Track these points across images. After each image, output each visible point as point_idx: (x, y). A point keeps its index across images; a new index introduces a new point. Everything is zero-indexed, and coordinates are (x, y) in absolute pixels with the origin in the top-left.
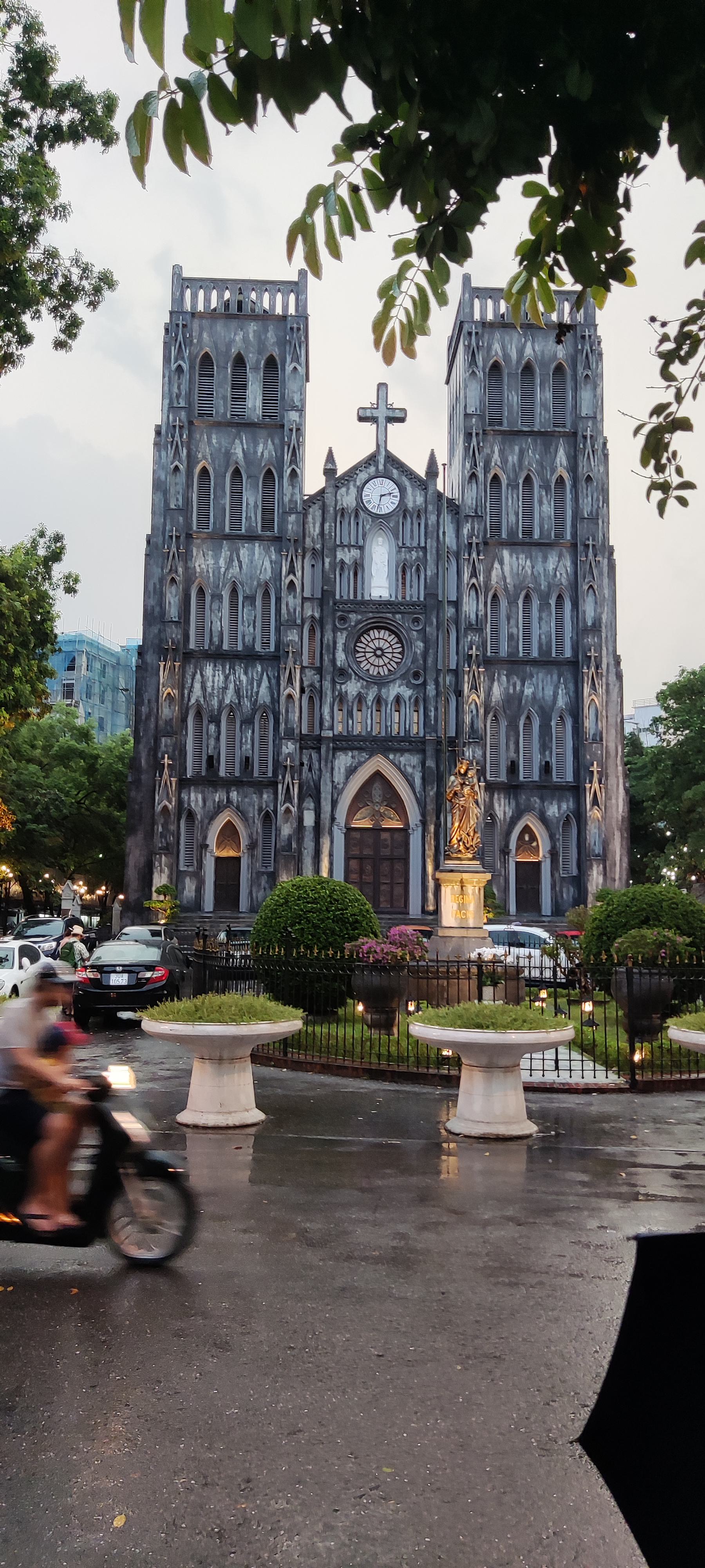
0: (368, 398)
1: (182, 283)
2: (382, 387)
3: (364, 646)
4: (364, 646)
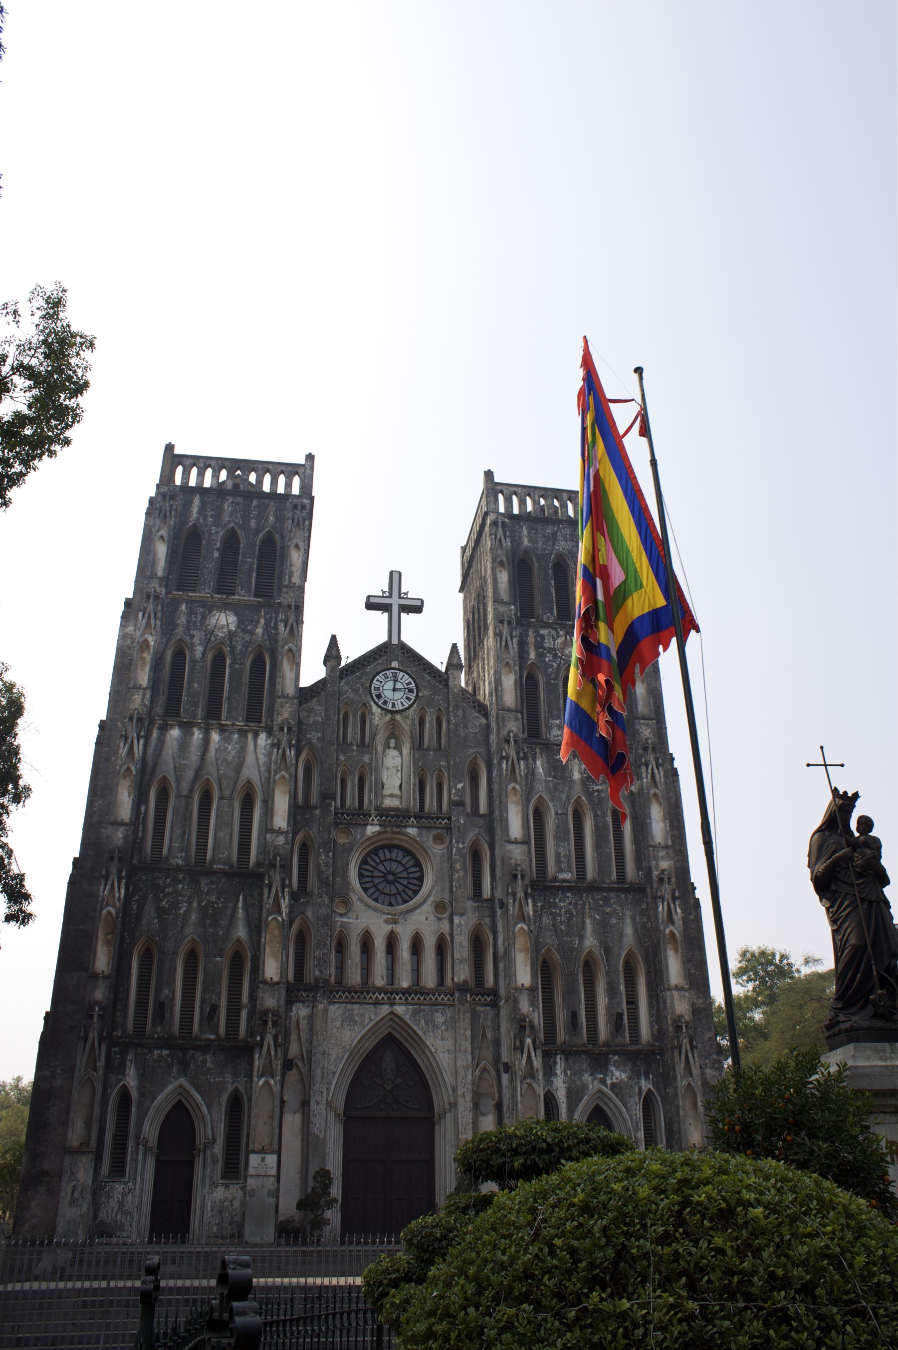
0: (379, 586)
1: (172, 459)
2: (395, 578)
3: (371, 869)
4: (371, 869)
